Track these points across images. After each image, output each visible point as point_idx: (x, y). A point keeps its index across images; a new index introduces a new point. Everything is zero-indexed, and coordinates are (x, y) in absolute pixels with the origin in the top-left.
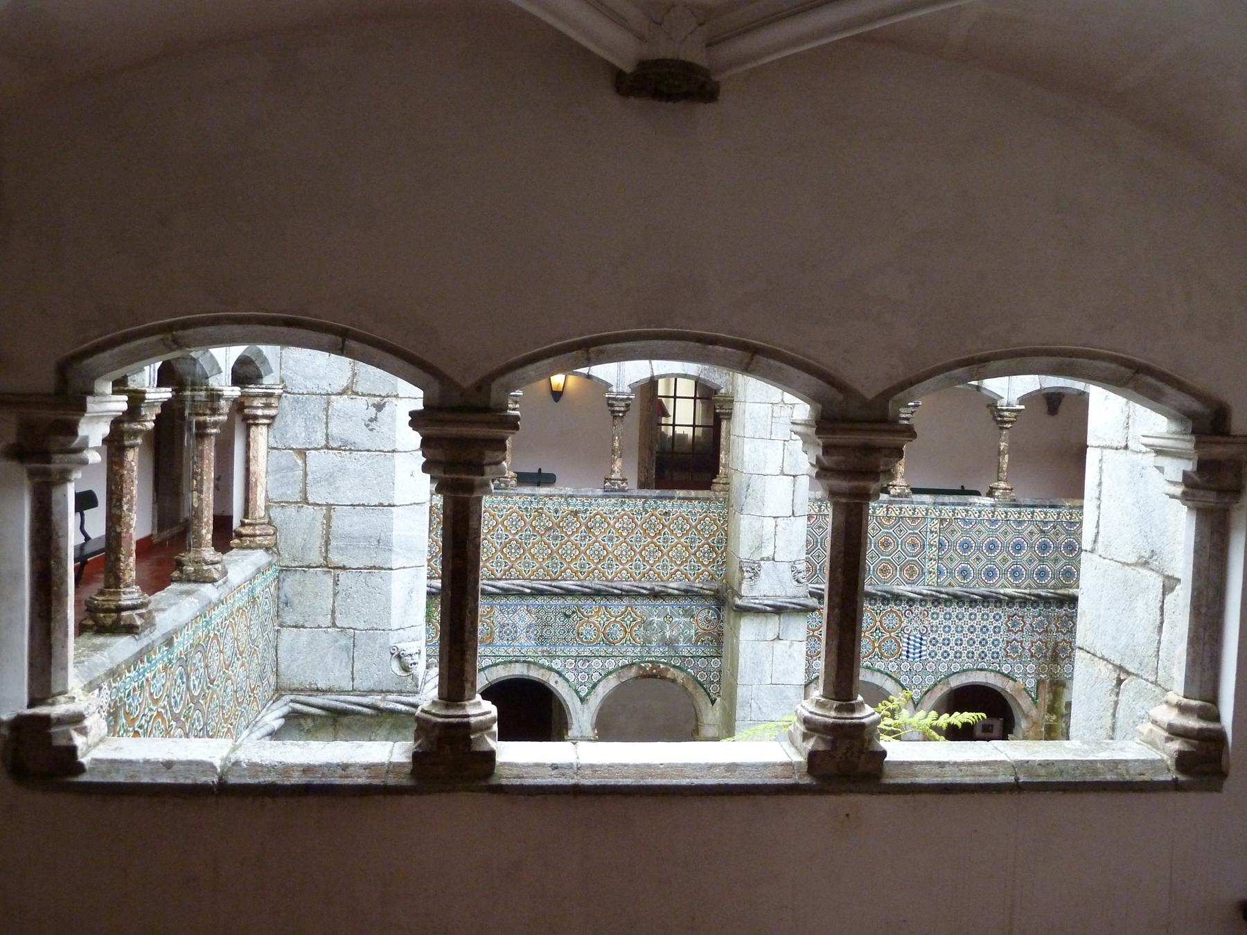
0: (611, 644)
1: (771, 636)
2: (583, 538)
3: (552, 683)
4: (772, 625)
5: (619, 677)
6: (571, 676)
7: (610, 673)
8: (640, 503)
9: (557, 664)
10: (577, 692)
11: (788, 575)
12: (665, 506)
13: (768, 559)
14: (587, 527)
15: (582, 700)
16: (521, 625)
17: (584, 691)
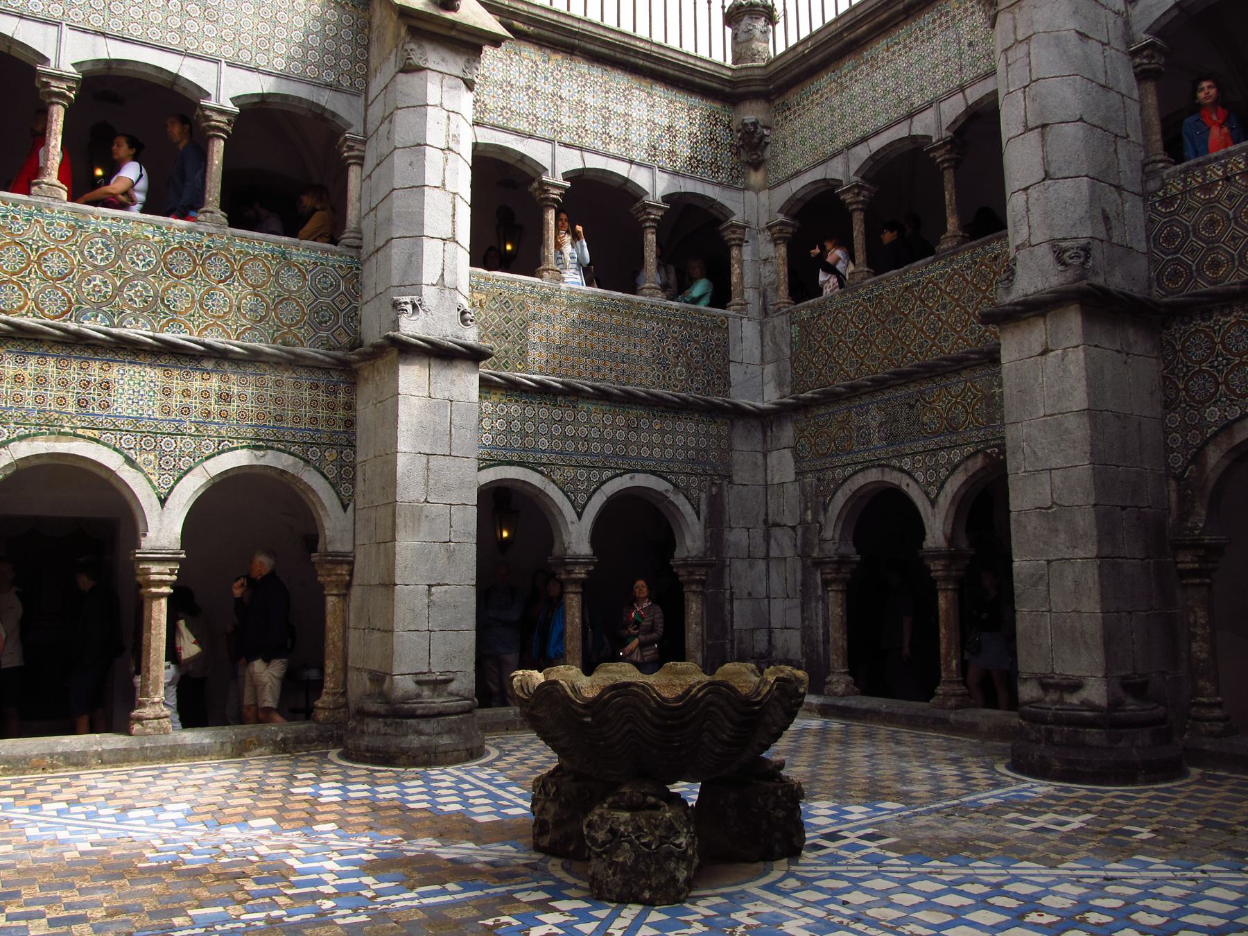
0: (953, 430)
1: (1039, 350)
2: (919, 314)
3: (904, 487)
4: (1035, 335)
5: (966, 470)
6: (919, 475)
7: (956, 467)
8: (967, 255)
9: (907, 463)
10: (927, 494)
11: (1050, 258)
12: (993, 249)
13: (1023, 245)
14: (922, 301)
15: (933, 503)
16: (874, 424)
17: (933, 490)
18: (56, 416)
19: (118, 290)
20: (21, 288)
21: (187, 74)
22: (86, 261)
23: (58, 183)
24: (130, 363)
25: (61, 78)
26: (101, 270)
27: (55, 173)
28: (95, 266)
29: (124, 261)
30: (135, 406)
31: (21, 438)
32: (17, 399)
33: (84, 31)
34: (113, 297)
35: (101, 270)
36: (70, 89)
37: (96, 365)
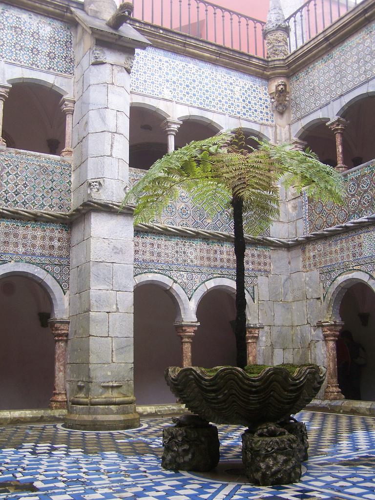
18: (347, 263)
19: (360, 201)
20: (333, 215)
21: (371, 90)
22: (349, 194)
23: (343, 166)
24: (366, 232)
25: (333, 124)
26: (353, 196)
27: (341, 162)
28: (352, 195)
29: (360, 188)
30: (370, 251)
31: (339, 275)
32: (336, 259)
33: (337, 99)
34: (358, 205)
35: (353, 196)
36: (338, 125)
37: (356, 237)
